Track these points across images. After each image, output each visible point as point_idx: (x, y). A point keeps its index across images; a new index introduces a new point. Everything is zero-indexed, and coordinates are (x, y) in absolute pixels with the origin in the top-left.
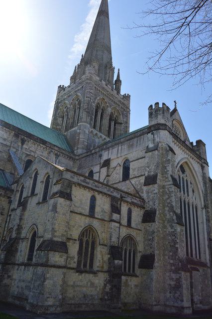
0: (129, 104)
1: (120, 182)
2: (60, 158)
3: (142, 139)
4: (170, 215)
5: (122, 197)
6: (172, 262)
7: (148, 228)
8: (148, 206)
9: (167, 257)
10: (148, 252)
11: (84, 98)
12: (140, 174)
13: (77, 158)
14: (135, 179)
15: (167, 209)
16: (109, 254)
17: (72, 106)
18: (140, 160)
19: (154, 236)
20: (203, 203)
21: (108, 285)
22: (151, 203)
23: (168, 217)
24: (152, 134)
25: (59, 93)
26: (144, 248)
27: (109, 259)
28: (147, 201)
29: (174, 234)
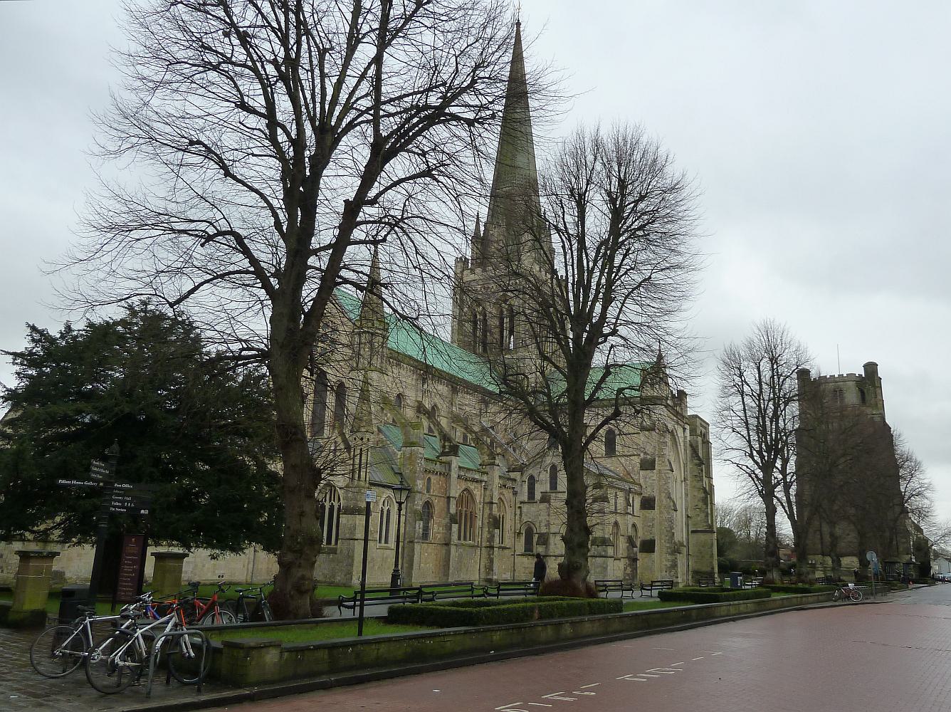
1: (602, 457)
6: (668, 545)
7: (647, 515)
9: (663, 541)
10: (648, 538)
20: (683, 475)
21: (628, 568)
22: (649, 489)
23: (664, 502)
26: (644, 534)
27: (628, 547)
28: (644, 487)
29: (671, 521)
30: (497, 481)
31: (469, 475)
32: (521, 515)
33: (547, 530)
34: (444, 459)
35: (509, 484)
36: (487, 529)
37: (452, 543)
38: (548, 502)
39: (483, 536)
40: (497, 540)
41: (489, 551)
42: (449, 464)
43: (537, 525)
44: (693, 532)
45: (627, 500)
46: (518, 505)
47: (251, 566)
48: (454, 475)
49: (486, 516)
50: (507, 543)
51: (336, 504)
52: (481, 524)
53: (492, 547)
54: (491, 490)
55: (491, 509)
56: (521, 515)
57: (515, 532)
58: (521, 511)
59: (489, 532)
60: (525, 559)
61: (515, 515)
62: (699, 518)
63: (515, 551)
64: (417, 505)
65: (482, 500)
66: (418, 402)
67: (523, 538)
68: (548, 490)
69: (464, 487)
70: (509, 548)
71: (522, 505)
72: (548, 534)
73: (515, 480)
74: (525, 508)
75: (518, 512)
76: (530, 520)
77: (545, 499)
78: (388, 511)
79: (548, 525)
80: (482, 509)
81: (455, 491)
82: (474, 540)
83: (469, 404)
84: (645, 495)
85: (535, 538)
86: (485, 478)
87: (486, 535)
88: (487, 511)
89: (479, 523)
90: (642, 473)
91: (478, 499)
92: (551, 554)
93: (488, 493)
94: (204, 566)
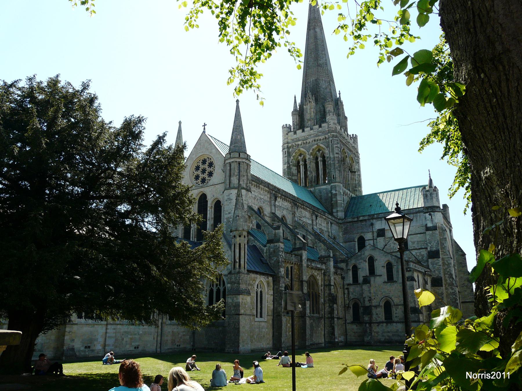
0: (358, 146)
2: (333, 225)
3: (418, 217)
4: (450, 280)
5: (425, 271)
7: (437, 291)
8: (434, 274)
11: (334, 155)
12: (420, 247)
13: (340, 221)
14: (416, 251)
15: (447, 276)
16: (428, 311)
17: (312, 156)
18: (419, 235)
19: (443, 296)
22: (437, 272)
23: (448, 281)
24: (430, 214)
25: (287, 134)
26: (436, 304)
28: (433, 270)
29: (454, 294)
30: (332, 270)
31: (313, 265)
32: (348, 293)
33: (370, 304)
34: (296, 252)
35: (339, 271)
36: (328, 305)
37: (307, 315)
38: (369, 282)
39: (325, 310)
40: (336, 312)
41: (331, 321)
42: (301, 256)
43: (362, 300)
44: (462, 302)
45: (424, 279)
46: (346, 287)
47: (159, 339)
48: (304, 264)
49: (326, 295)
50: (341, 315)
51: (222, 289)
52: (323, 301)
53: (333, 318)
54: (329, 275)
55: (330, 290)
56: (348, 293)
57: (345, 306)
58: (348, 292)
59: (330, 307)
60: (354, 327)
61: (344, 294)
62: (466, 293)
63: (346, 320)
64: (282, 287)
65: (323, 283)
66: (273, 213)
67: (351, 311)
68: (368, 274)
69: (310, 273)
70: (341, 318)
71: (349, 287)
72: (371, 306)
73: (342, 269)
74: (351, 289)
75: (346, 291)
76: (356, 297)
77: (366, 281)
78: (261, 292)
79: (370, 300)
80: (323, 290)
81: (305, 278)
82: (319, 313)
83: (305, 217)
84: (434, 276)
85: (361, 310)
86: (324, 267)
87: (327, 309)
88: (327, 291)
89: (322, 300)
90: (430, 260)
91: (320, 282)
92: (374, 321)
93: (326, 278)
94: (123, 339)
